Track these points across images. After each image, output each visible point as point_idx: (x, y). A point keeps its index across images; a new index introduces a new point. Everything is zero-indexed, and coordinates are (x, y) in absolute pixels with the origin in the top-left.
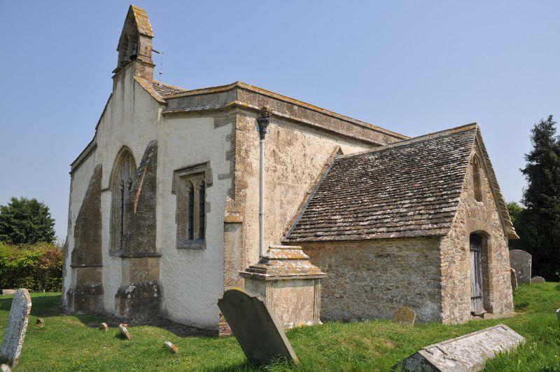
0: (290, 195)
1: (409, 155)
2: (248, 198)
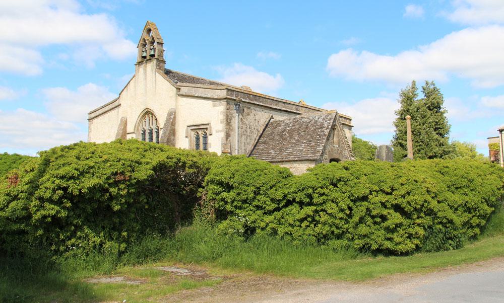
0: (248, 140)
1: (306, 122)
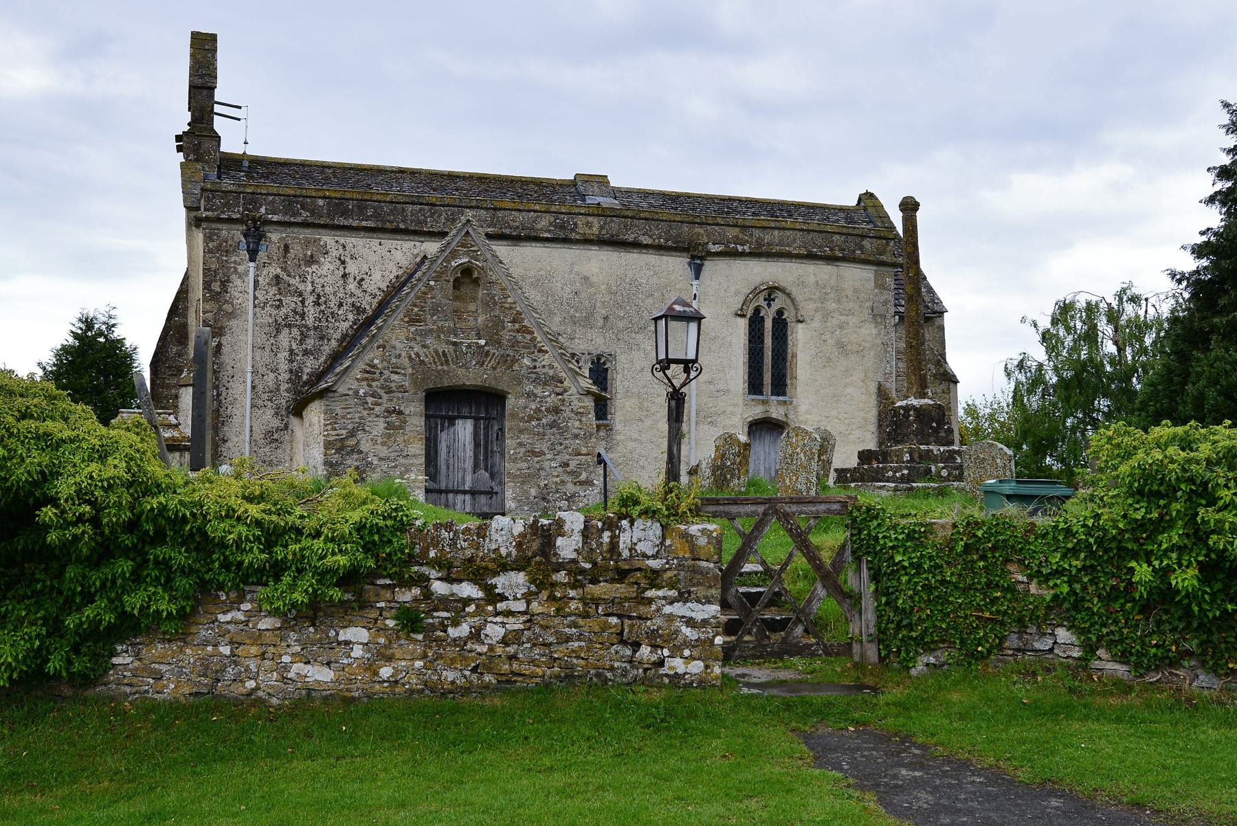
2: (226, 349)
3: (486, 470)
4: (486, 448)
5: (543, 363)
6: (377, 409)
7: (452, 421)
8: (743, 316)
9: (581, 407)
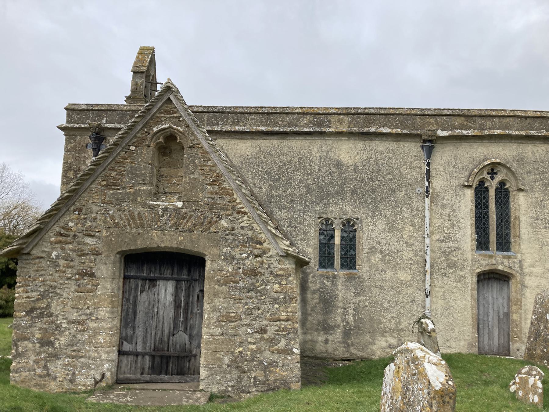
3: (185, 332)
4: (186, 309)
5: (242, 224)
6: (69, 271)
7: (153, 281)
8: (469, 187)
9: (281, 269)
